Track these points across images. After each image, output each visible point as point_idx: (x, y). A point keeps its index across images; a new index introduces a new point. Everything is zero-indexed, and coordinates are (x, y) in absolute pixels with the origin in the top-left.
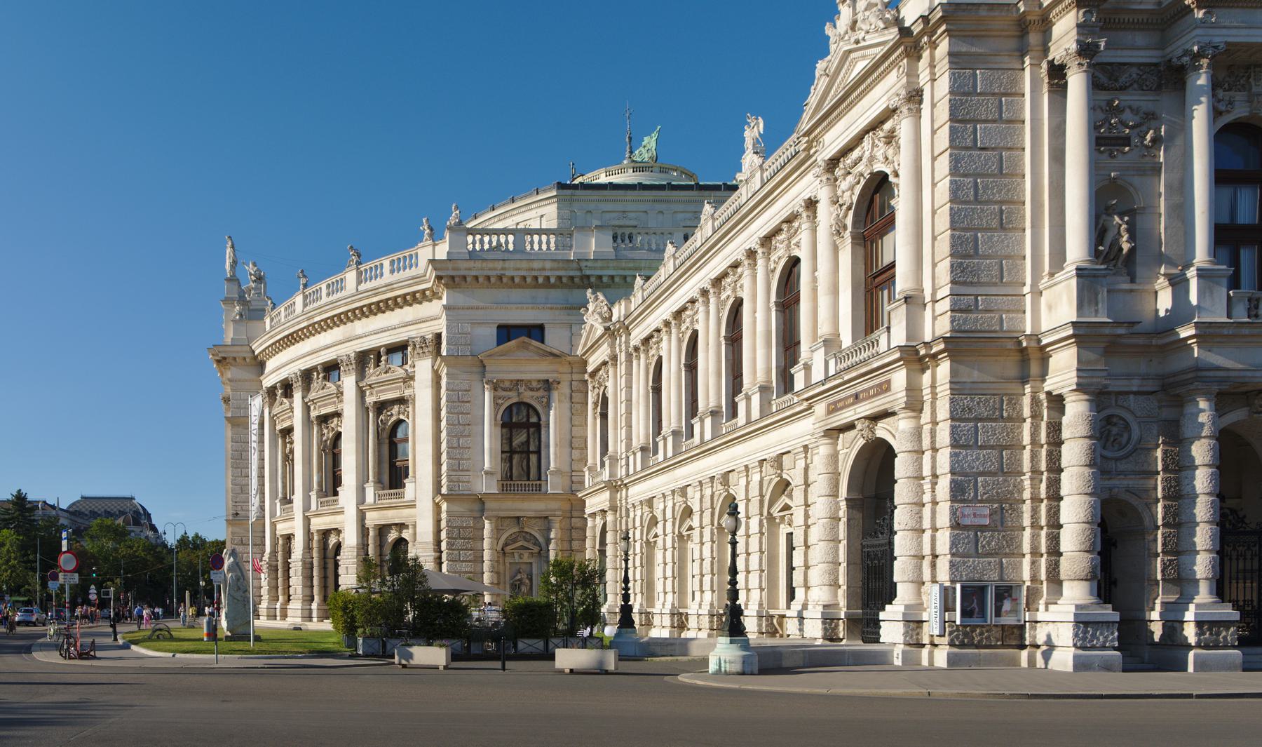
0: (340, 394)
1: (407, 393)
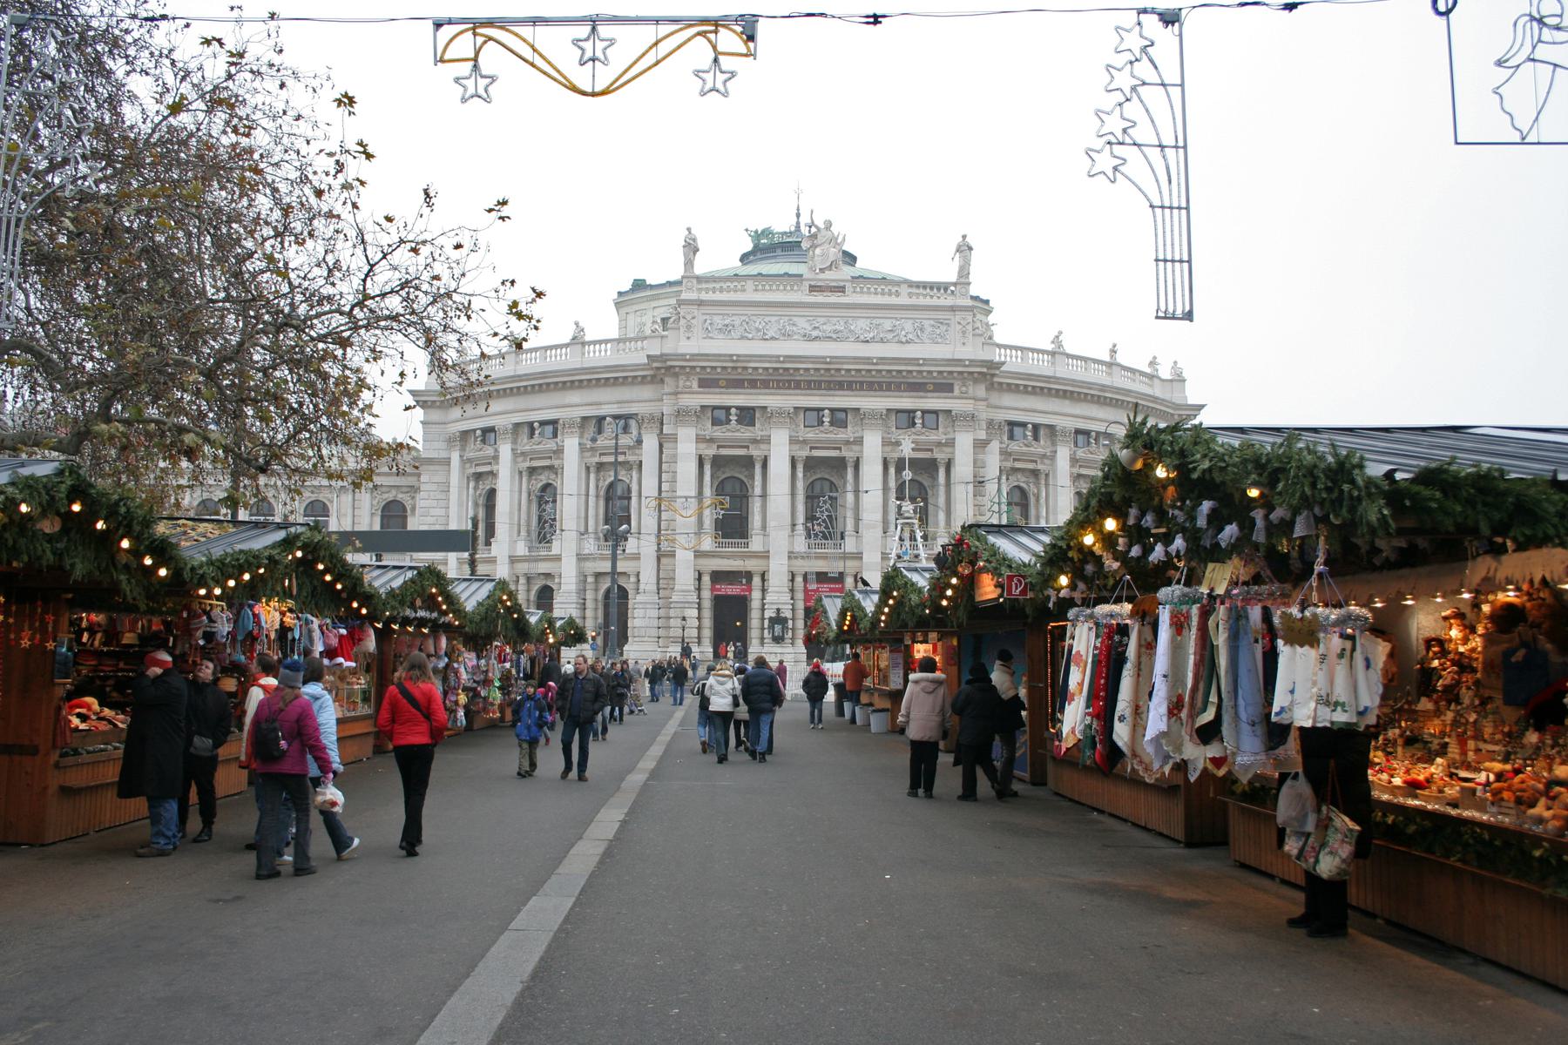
0: (559, 452)
1: (630, 458)
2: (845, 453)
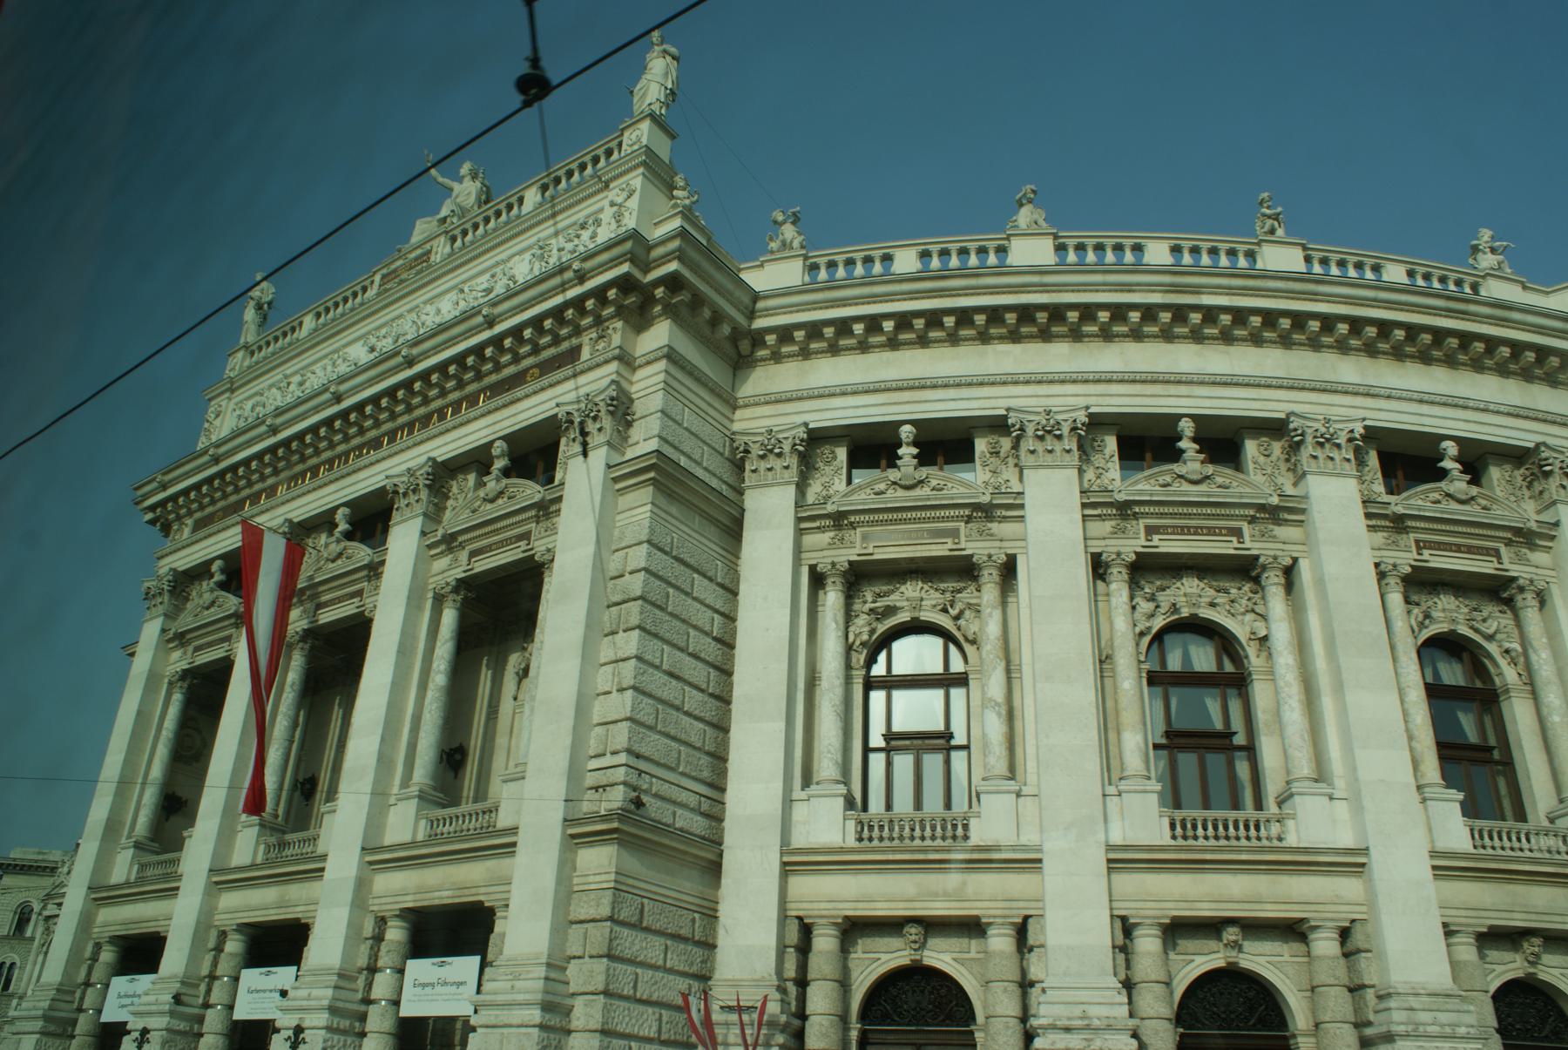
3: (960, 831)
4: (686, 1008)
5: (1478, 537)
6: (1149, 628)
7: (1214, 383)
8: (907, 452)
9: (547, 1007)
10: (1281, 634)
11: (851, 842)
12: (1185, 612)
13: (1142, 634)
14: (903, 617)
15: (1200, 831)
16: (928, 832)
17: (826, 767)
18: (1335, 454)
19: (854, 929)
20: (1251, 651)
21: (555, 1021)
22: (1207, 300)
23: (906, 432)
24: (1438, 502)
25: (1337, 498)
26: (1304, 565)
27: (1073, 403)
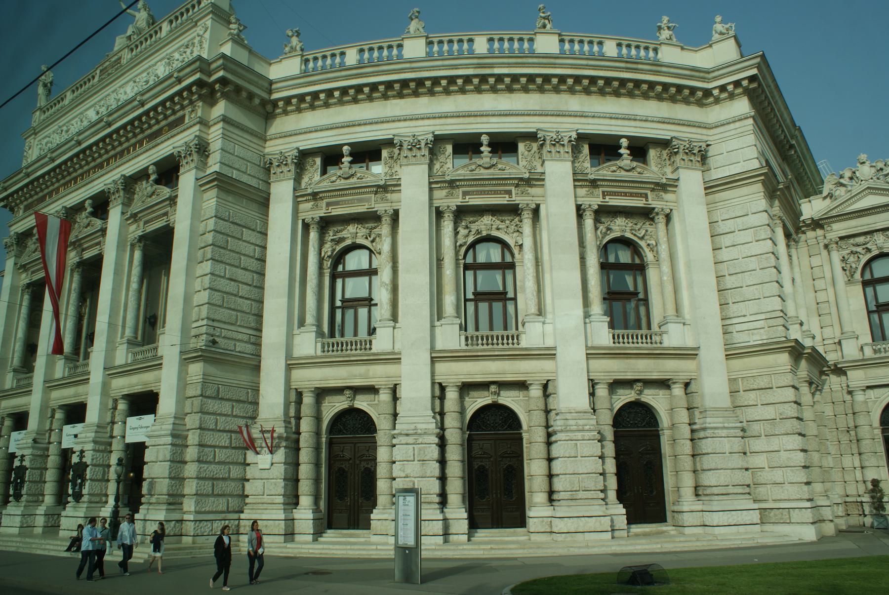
2: (517, 198)
3: (368, 346)
4: (241, 432)
5: (637, 187)
6: (465, 243)
7: (500, 115)
8: (346, 159)
9: (174, 436)
10: (528, 242)
11: (319, 353)
12: (484, 233)
13: (461, 246)
14: (348, 242)
15: (505, 341)
16: (354, 347)
17: (310, 319)
18: (561, 150)
19: (321, 393)
20: (516, 251)
21: (179, 442)
22: (497, 71)
23: (346, 149)
24: (614, 171)
25: (558, 172)
26: (542, 208)
27: (425, 130)
